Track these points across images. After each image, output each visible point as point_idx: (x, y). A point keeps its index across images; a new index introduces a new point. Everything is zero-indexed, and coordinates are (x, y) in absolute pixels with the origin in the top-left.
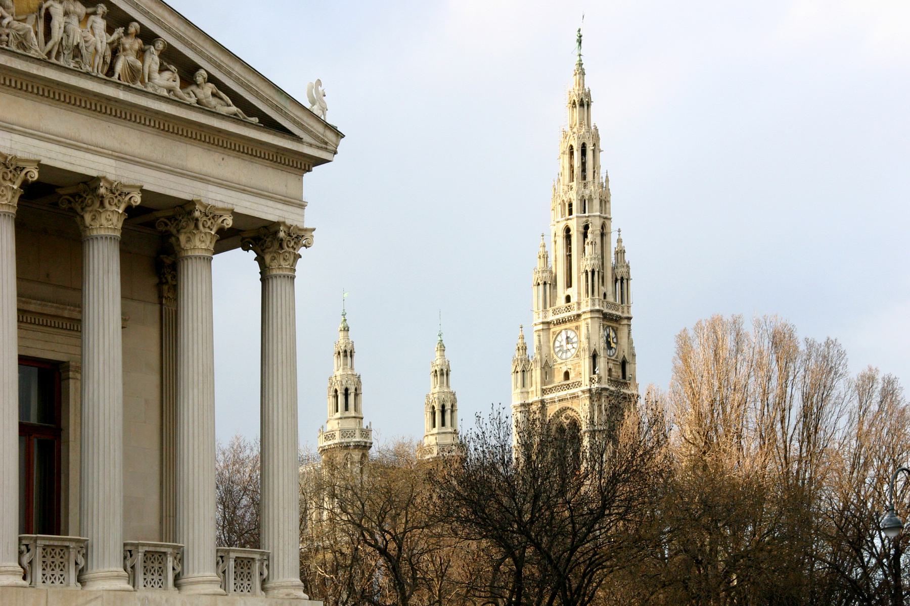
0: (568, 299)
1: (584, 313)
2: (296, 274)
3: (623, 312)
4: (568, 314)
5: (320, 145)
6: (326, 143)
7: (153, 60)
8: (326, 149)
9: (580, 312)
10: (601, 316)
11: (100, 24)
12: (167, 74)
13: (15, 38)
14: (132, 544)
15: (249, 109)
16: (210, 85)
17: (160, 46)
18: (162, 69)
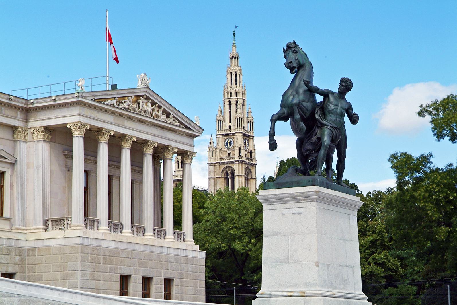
0: (230, 127)
1: (236, 133)
2: (192, 163)
3: (251, 134)
4: (230, 133)
5: (198, 132)
6: (200, 132)
7: (161, 111)
8: (200, 133)
9: (234, 132)
10: (243, 135)
11: (150, 104)
12: (164, 116)
13: (133, 109)
14: (155, 228)
15: (182, 124)
16: (173, 118)
17: (162, 109)
18: (163, 114)
